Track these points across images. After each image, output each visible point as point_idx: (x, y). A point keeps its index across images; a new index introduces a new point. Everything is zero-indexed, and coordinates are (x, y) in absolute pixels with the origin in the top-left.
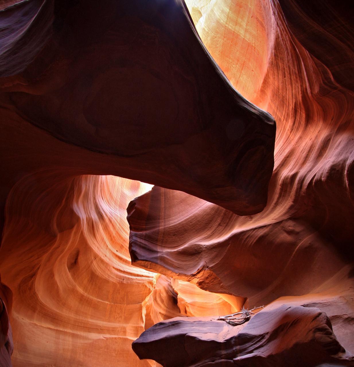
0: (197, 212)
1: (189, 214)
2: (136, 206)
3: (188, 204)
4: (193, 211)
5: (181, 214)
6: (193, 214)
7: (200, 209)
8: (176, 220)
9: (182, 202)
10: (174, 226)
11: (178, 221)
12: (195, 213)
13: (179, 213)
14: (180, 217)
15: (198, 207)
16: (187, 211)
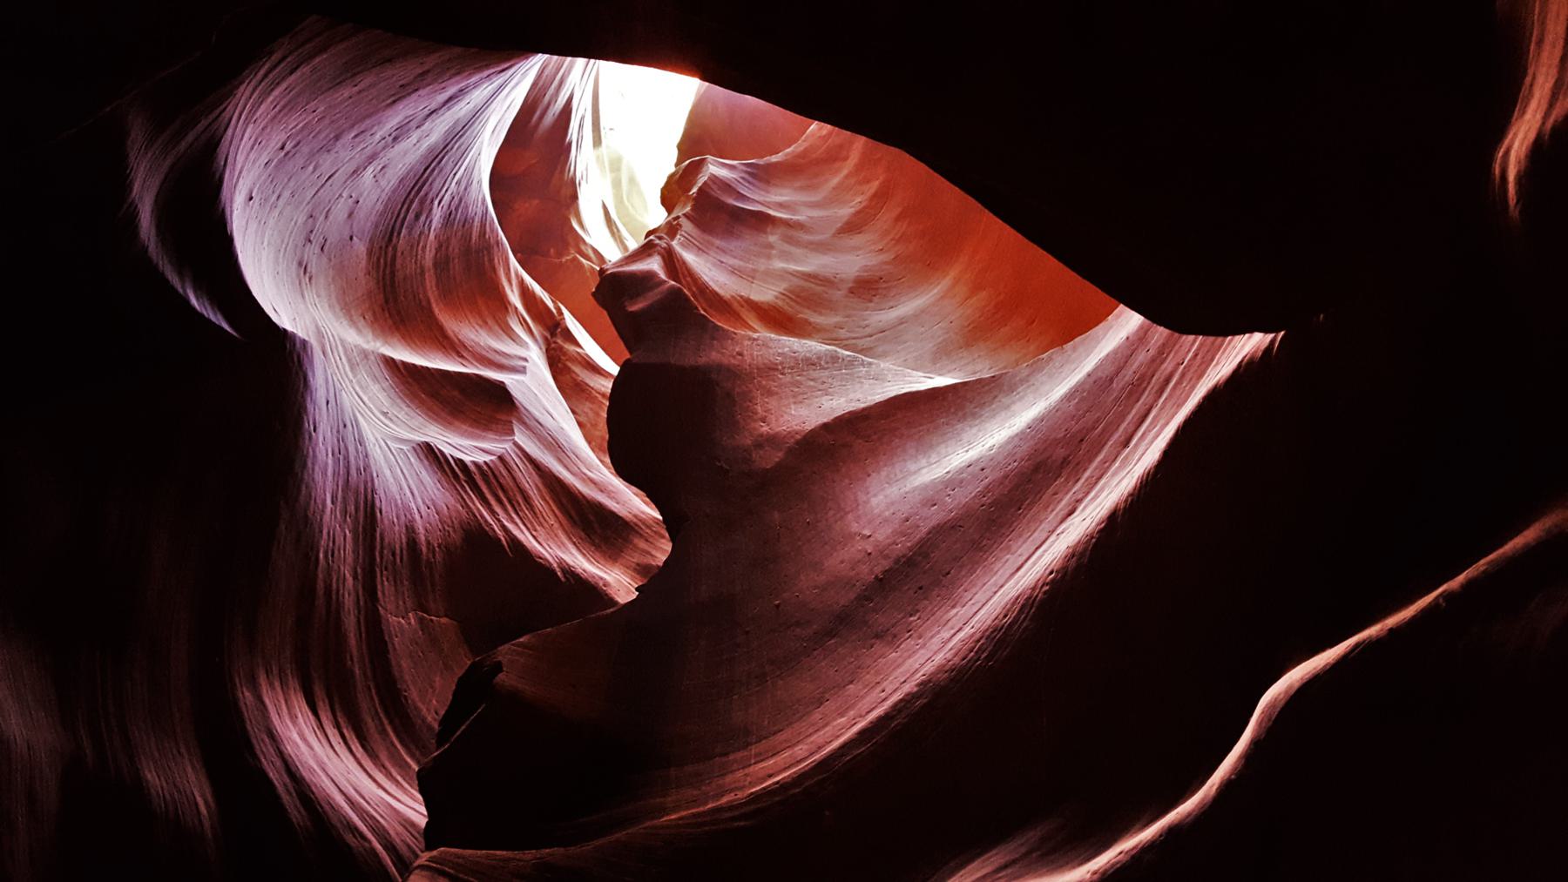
0: (939, 659)
1: (888, 690)
2: (501, 678)
3: (877, 636)
4: (913, 663)
5: (829, 706)
6: (919, 678)
7: (961, 635)
8: (800, 750)
9: (831, 634)
10: (783, 787)
11: (812, 754)
12: (929, 668)
13: (820, 702)
14: (826, 725)
15: (946, 635)
16: (878, 673)
